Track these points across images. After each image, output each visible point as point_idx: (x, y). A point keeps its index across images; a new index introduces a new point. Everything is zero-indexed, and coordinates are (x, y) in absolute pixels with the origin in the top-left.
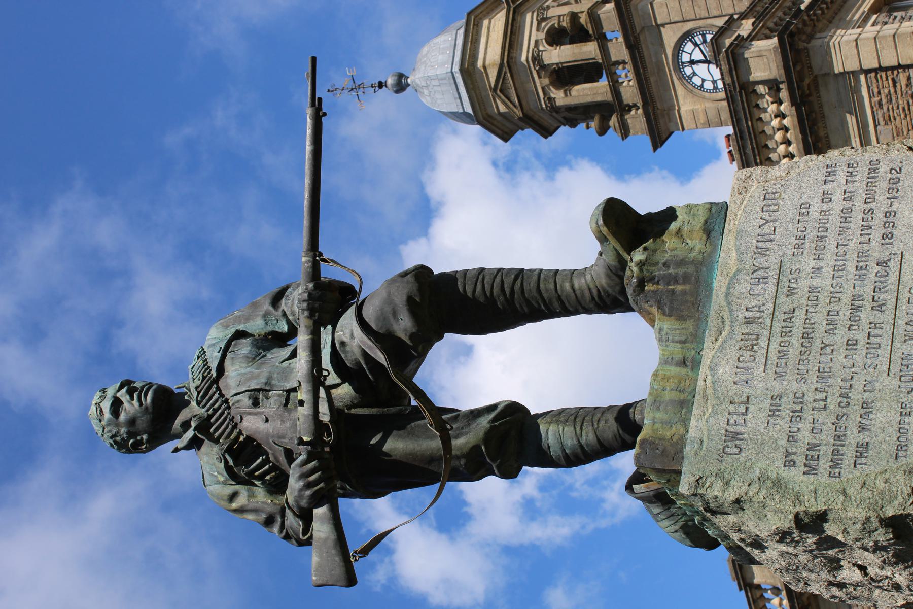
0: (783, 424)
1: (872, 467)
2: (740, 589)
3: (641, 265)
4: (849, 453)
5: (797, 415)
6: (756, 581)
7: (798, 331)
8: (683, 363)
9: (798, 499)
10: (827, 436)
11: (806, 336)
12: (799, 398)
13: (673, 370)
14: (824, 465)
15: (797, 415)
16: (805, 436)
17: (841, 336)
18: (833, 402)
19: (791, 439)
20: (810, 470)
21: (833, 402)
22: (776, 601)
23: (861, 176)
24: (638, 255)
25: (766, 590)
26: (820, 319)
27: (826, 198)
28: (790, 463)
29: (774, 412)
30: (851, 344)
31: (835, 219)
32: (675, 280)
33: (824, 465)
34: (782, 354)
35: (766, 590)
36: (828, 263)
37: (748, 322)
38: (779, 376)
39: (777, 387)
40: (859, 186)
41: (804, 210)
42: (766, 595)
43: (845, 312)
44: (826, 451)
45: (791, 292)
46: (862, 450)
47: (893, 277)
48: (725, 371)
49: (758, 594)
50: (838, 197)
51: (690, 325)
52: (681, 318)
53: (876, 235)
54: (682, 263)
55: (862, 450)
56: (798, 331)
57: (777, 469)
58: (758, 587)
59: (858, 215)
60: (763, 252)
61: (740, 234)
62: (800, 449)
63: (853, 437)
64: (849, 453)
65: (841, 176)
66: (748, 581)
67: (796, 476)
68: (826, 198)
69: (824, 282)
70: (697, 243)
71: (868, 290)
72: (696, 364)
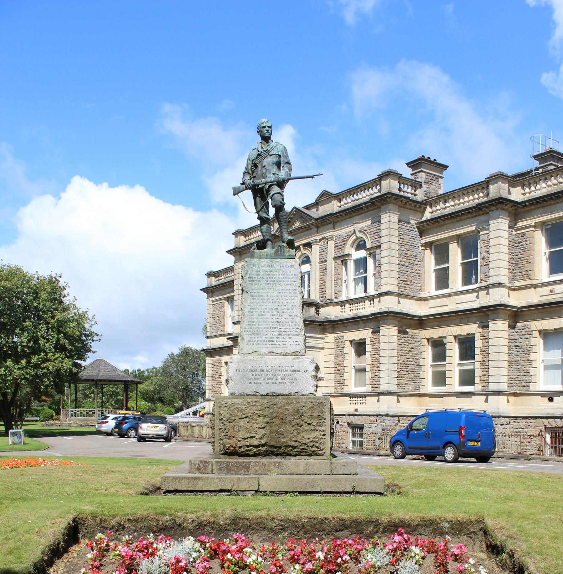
0: (256, 273)
1: (249, 286)
2: (378, 176)
3: (283, 246)
4: (251, 283)
5: (257, 275)
6: (382, 182)
7: (270, 273)
8: (267, 255)
9: (245, 276)
10: (254, 279)
11: (269, 275)
12: (259, 275)
13: (266, 254)
14: (250, 279)
15: (257, 275)
16: (254, 276)
17: (269, 279)
18: (259, 280)
19: (253, 274)
20: (249, 278)
21: (259, 280)
22: (376, 191)
23: (295, 280)
24: (285, 245)
25: (380, 186)
26: (272, 276)
27: (292, 275)
28: (250, 275)
29: (257, 271)
30: (268, 281)
31: (288, 276)
32: (281, 251)
33: (250, 279)
34: (266, 271)
35: (380, 186)
36: (280, 276)
37: (272, 265)
38: (263, 271)
39: (261, 271)
40: (293, 280)
41: (290, 271)
42: (378, 186)
43: (272, 280)
44: (252, 280)
45: (276, 271)
46: (252, 284)
47: (278, 286)
48: (264, 263)
49: (378, 183)
50: (292, 276)
51: (274, 255)
52: (274, 254)
53: (285, 283)
54: (284, 252)
55: (252, 284)
56: (270, 273)
57: (249, 273)
58: (381, 183)
59: (287, 280)
60: (283, 266)
61: (287, 262)
62: (252, 276)
63: (254, 283)
64: (251, 283)
65: (295, 277)
66: (382, 179)
67: (248, 276)
68: (292, 275)
69: (278, 276)
70: (287, 254)
71: (276, 282)
72: (267, 258)
